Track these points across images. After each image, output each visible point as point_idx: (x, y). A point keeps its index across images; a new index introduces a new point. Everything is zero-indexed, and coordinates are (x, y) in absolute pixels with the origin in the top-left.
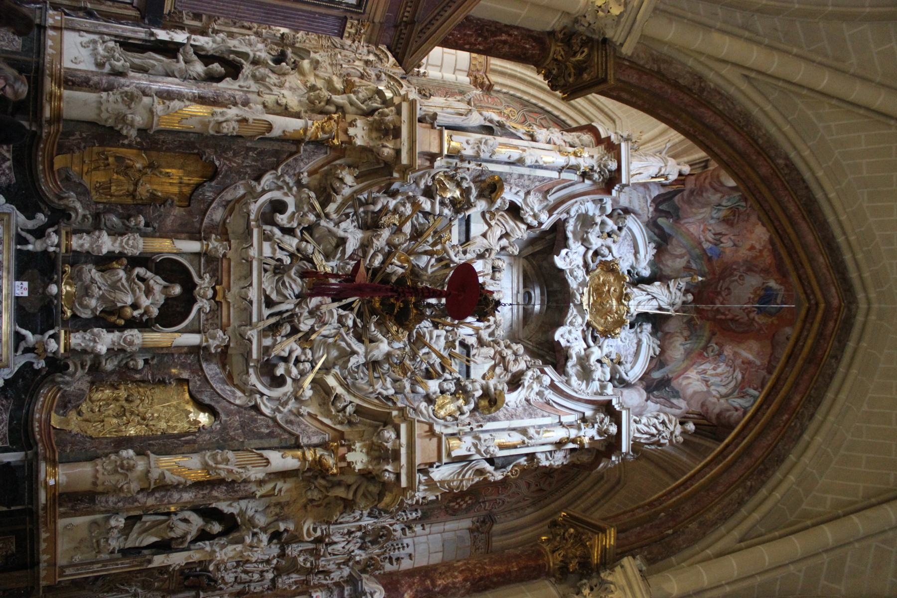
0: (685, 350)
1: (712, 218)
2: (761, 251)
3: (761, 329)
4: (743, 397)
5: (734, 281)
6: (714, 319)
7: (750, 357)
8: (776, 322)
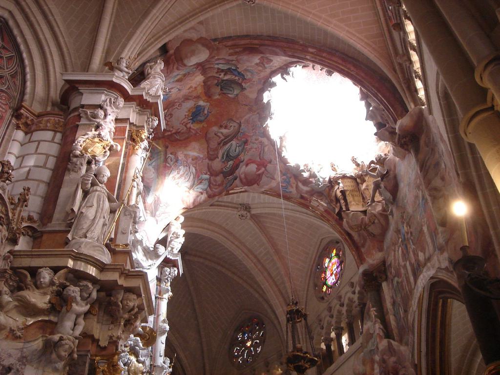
0: (154, 167)
1: (169, 83)
2: (195, 88)
3: (197, 133)
4: (200, 183)
5: (174, 109)
6: (164, 137)
7: (195, 154)
8: (206, 125)
